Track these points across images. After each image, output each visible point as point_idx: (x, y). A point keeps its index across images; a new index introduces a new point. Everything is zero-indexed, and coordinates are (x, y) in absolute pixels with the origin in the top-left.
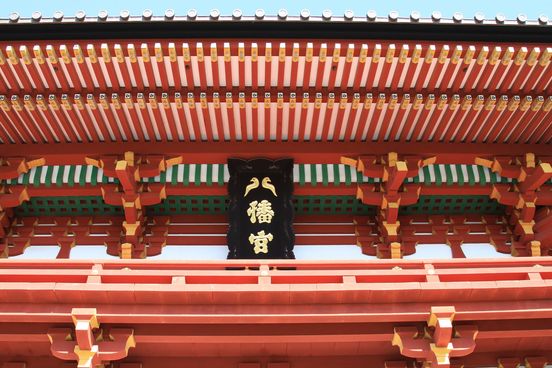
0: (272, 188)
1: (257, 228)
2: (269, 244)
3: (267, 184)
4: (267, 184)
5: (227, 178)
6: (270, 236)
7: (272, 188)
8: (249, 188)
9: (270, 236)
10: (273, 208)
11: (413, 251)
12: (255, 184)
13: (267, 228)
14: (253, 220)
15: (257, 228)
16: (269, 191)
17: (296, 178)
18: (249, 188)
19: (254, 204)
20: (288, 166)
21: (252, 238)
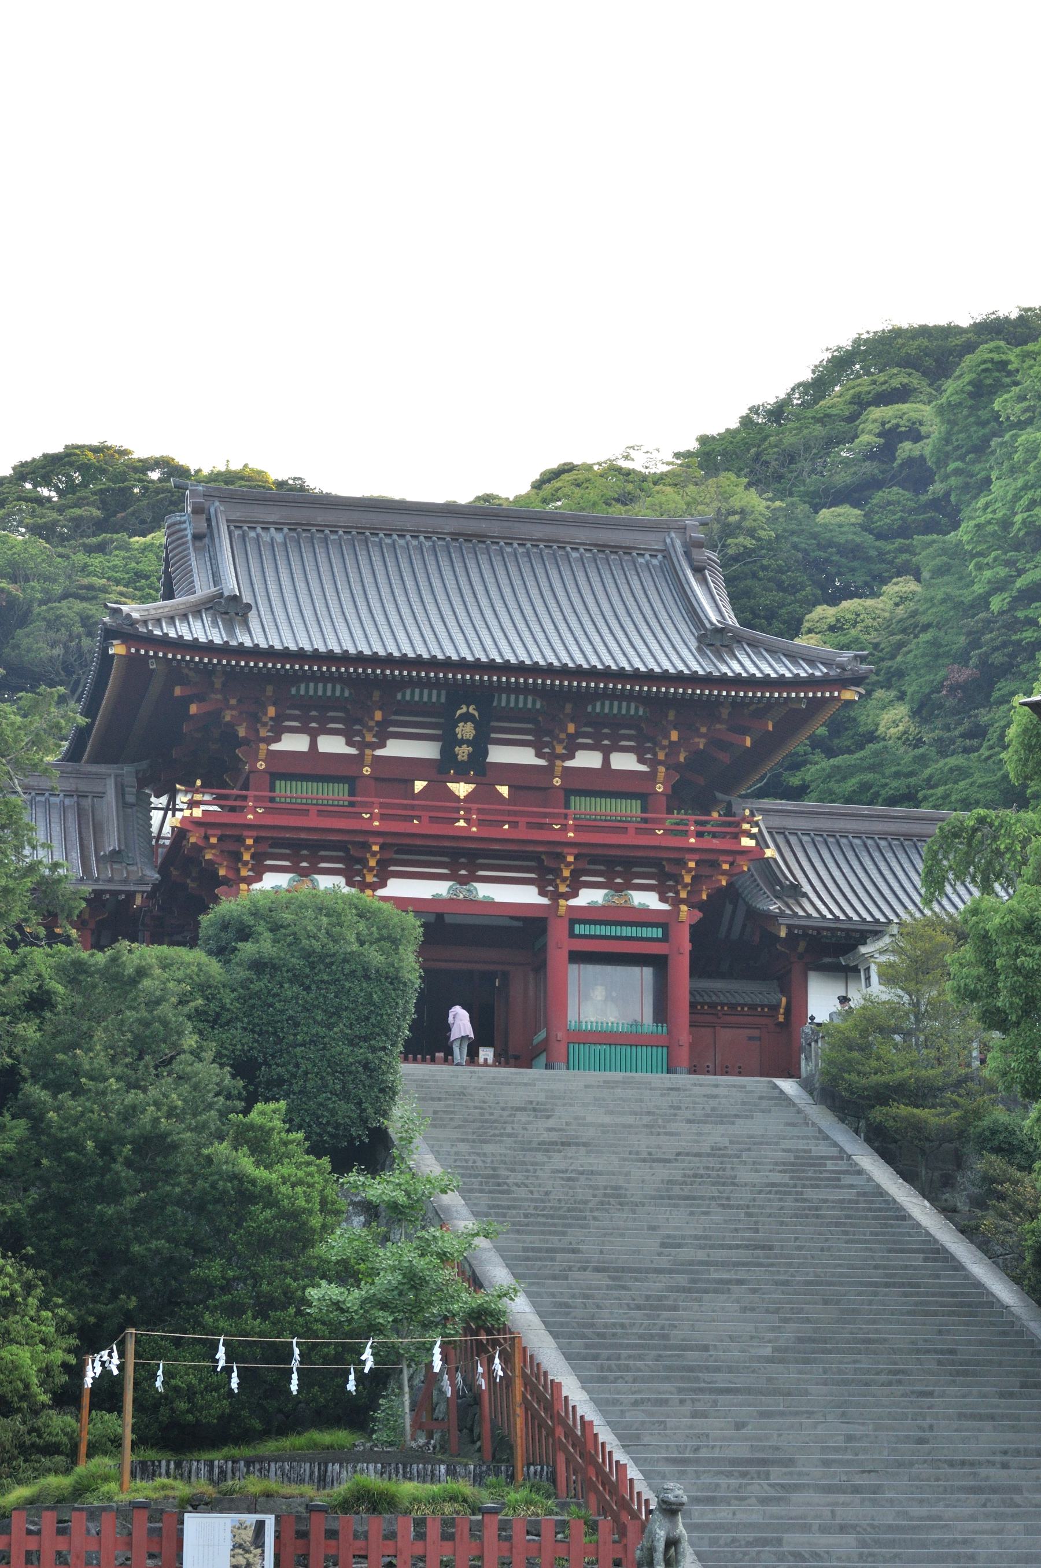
0: (476, 714)
1: (462, 742)
2: (469, 755)
3: (471, 710)
5: (443, 700)
7: (476, 714)
8: (459, 712)
9: (470, 749)
10: (475, 729)
12: (464, 709)
13: (468, 743)
14: (459, 736)
15: (462, 742)
16: (473, 716)
18: (459, 712)
19: (461, 724)
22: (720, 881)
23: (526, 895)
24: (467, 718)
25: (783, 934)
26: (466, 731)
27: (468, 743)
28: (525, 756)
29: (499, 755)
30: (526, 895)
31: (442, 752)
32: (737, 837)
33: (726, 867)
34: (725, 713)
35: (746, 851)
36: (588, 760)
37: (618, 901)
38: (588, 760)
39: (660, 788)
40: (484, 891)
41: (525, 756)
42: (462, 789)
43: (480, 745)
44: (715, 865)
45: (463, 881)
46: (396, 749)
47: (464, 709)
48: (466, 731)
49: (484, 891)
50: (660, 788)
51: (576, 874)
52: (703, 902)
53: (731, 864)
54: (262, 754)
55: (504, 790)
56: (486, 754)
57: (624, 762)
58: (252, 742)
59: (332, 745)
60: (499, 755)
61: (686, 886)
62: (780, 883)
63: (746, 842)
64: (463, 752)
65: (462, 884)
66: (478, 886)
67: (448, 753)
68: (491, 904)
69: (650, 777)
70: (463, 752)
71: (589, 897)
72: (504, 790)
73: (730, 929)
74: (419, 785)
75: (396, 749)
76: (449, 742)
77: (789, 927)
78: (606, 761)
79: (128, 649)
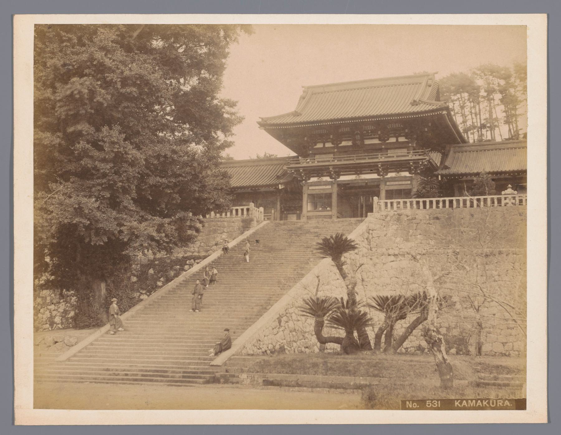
3: (358, 132)
4: (358, 132)
12: (356, 132)
26: (358, 137)
30: (375, 176)
36: (393, 140)
43: (362, 140)
47: (356, 132)
56: (364, 142)
71: (390, 175)
76: (354, 141)
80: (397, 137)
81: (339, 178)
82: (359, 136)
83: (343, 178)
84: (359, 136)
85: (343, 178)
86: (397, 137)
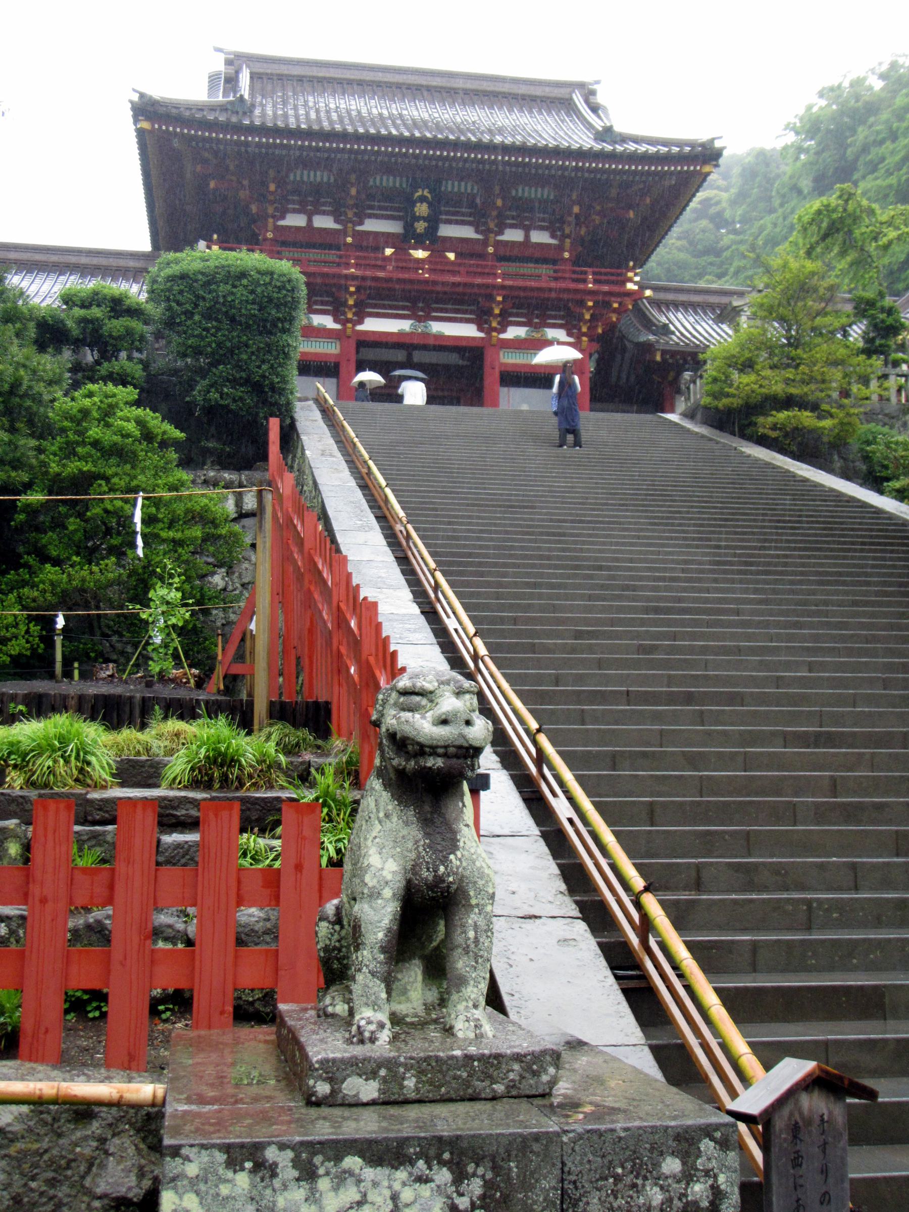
0: (429, 196)
1: (418, 219)
3: (426, 193)
4: (426, 193)
6: (426, 224)
7: (429, 196)
9: (426, 224)
11: (503, 234)
12: (419, 193)
13: (425, 219)
15: (418, 219)
17: (443, 189)
20: (439, 181)
21: (416, 225)
22: (610, 318)
23: (468, 331)
24: (423, 199)
25: (658, 358)
26: (422, 209)
27: (425, 219)
28: (467, 232)
29: (447, 231)
30: (468, 331)
31: (405, 228)
32: (623, 283)
33: (616, 305)
34: (614, 192)
35: (630, 294)
36: (513, 235)
37: (537, 335)
38: (513, 235)
39: (566, 255)
40: (438, 328)
41: (467, 232)
42: (420, 254)
43: (433, 222)
44: (607, 304)
45: (419, 319)
46: (371, 225)
47: (419, 193)
48: (422, 209)
49: (438, 328)
50: (566, 255)
51: (504, 314)
52: (599, 336)
53: (620, 304)
54: (270, 226)
55: (451, 256)
57: (540, 237)
58: (263, 217)
59: (324, 222)
60: (447, 231)
61: (586, 322)
62: (655, 325)
63: (630, 286)
64: (421, 226)
65: (420, 321)
66: (431, 323)
67: (409, 227)
68: (440, 337)
69: (560, 248)
70: (421, 226)
72: (451, 256)
73: (619, 378)
74: (389, 251)
75: (371, 225)
76: (409, 220)
77: (664, 352)
78: (527, 236)
79: (153, 126)
80: (527, 230)
81: (361, 322)
82: (425, 205)
83: (373, 325)
84: (425, 205)
85: (373, 325)
86: (527, 230)
